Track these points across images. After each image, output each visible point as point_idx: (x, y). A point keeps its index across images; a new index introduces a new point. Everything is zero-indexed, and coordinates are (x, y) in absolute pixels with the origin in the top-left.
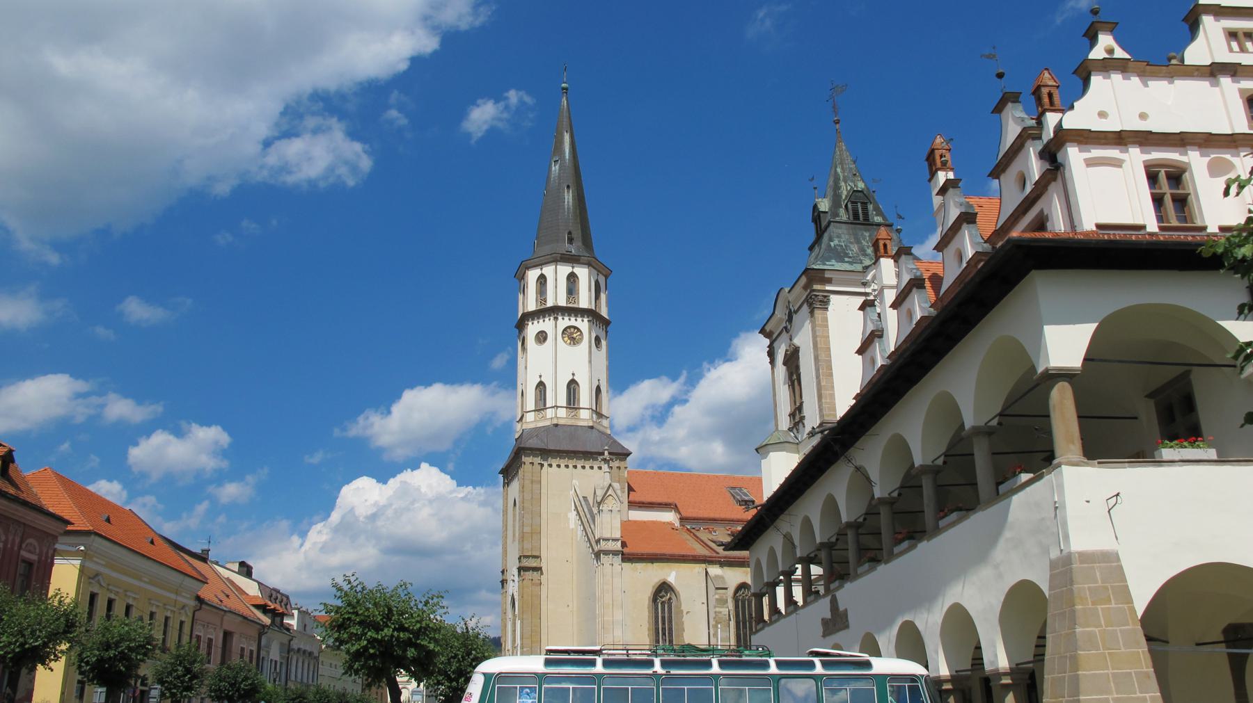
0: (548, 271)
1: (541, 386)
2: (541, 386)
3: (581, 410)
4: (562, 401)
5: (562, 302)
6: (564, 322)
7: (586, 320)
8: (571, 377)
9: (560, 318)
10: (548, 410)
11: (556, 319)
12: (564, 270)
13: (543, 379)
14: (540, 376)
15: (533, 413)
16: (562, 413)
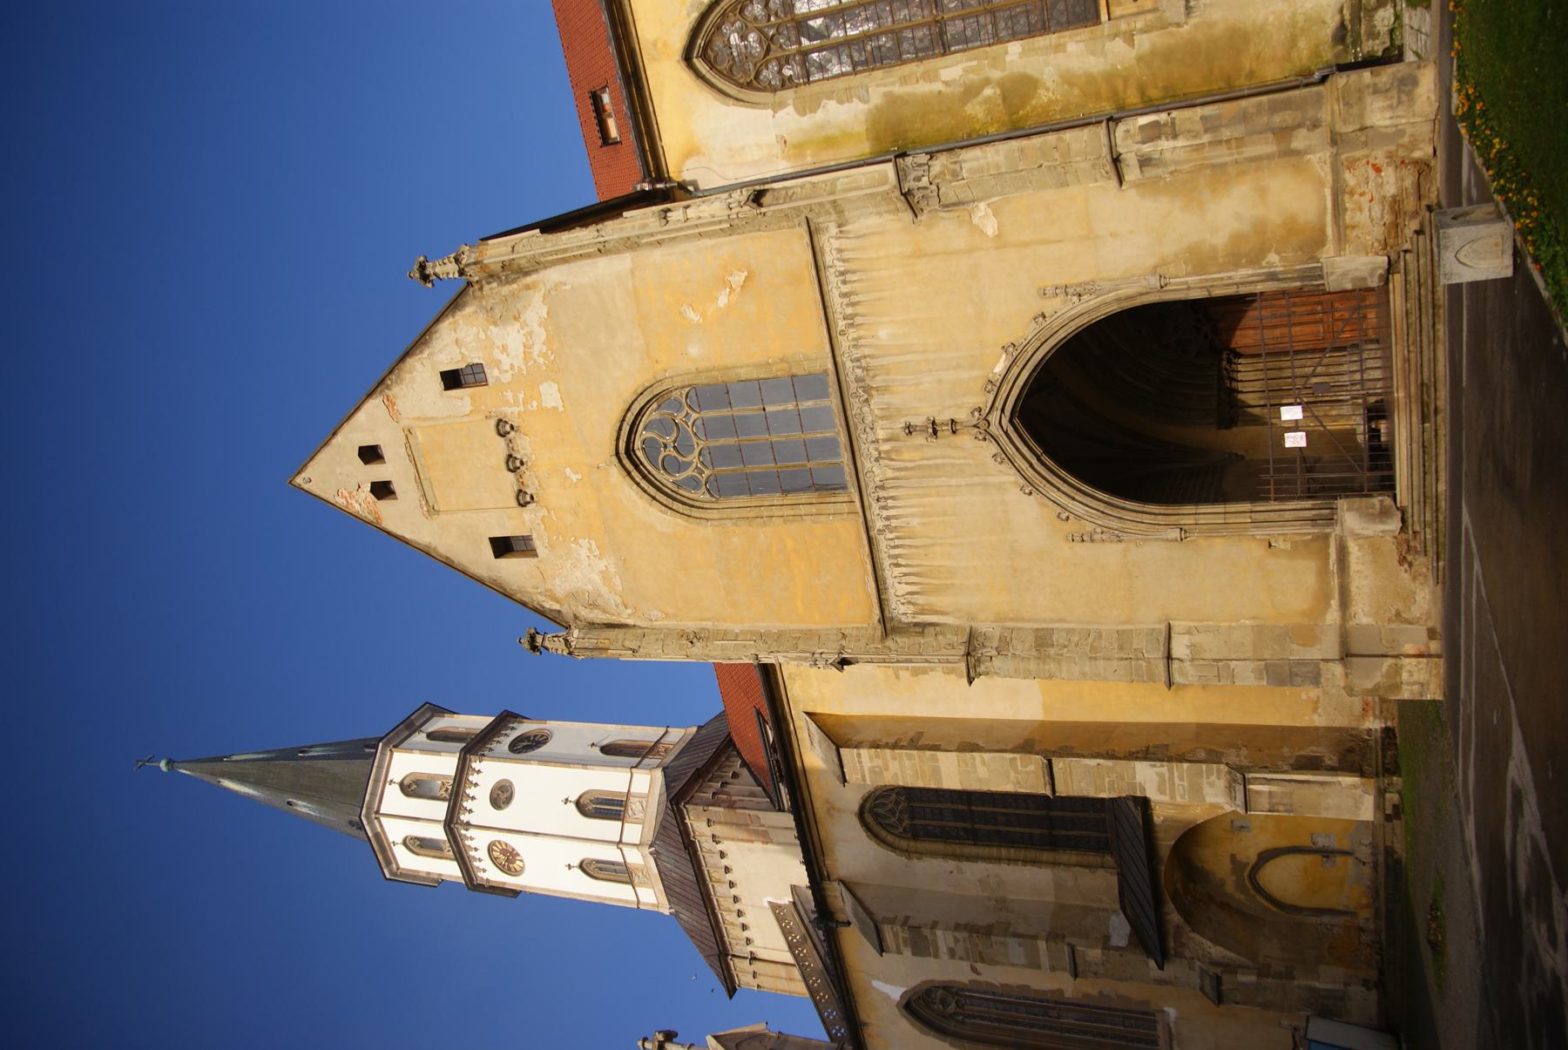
0: (395, 831)
1: (590, 868)
2: (590, 868)
3: (632, 790)
4: (609, 828)
5: (440, 809)
6: (478, 808)
7: (476, 765)
8: (573, 807)
9: (464, 817)
10: (628, 861)
11: (468, 825)
12: (393, 800)
13: (576, 863)
14: (570, 867)
15: (637, 888)
16: (633, 832)
